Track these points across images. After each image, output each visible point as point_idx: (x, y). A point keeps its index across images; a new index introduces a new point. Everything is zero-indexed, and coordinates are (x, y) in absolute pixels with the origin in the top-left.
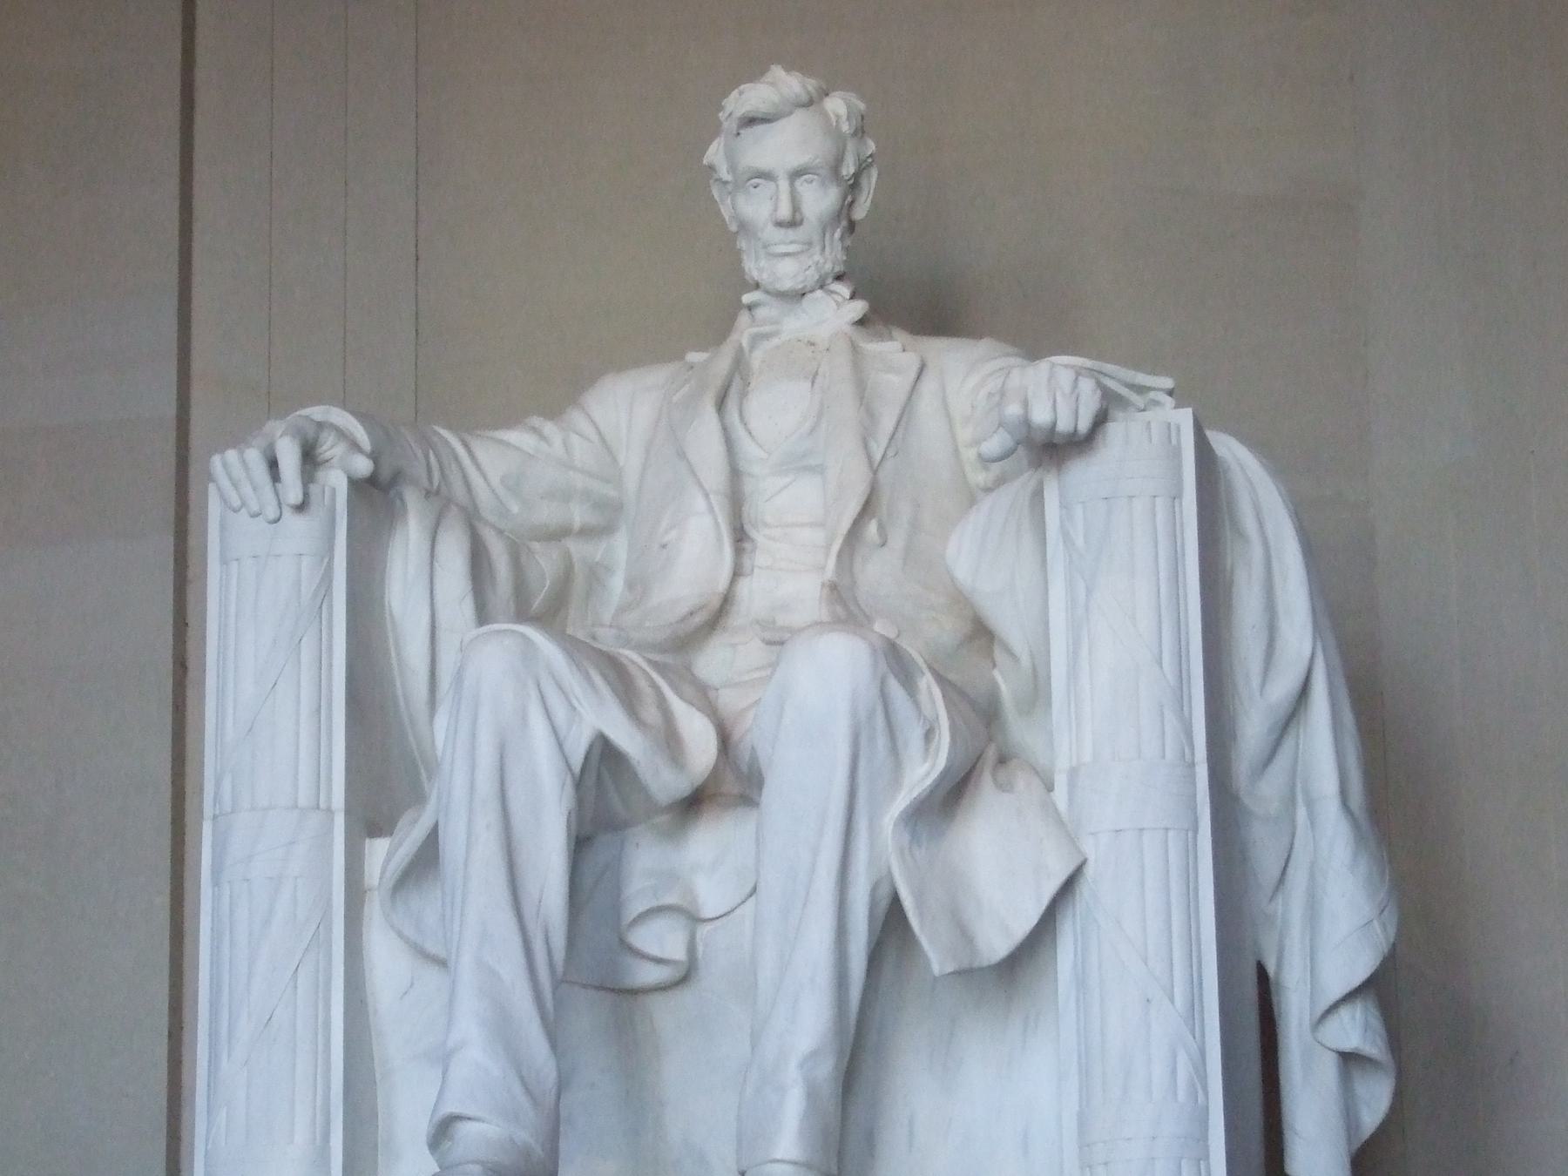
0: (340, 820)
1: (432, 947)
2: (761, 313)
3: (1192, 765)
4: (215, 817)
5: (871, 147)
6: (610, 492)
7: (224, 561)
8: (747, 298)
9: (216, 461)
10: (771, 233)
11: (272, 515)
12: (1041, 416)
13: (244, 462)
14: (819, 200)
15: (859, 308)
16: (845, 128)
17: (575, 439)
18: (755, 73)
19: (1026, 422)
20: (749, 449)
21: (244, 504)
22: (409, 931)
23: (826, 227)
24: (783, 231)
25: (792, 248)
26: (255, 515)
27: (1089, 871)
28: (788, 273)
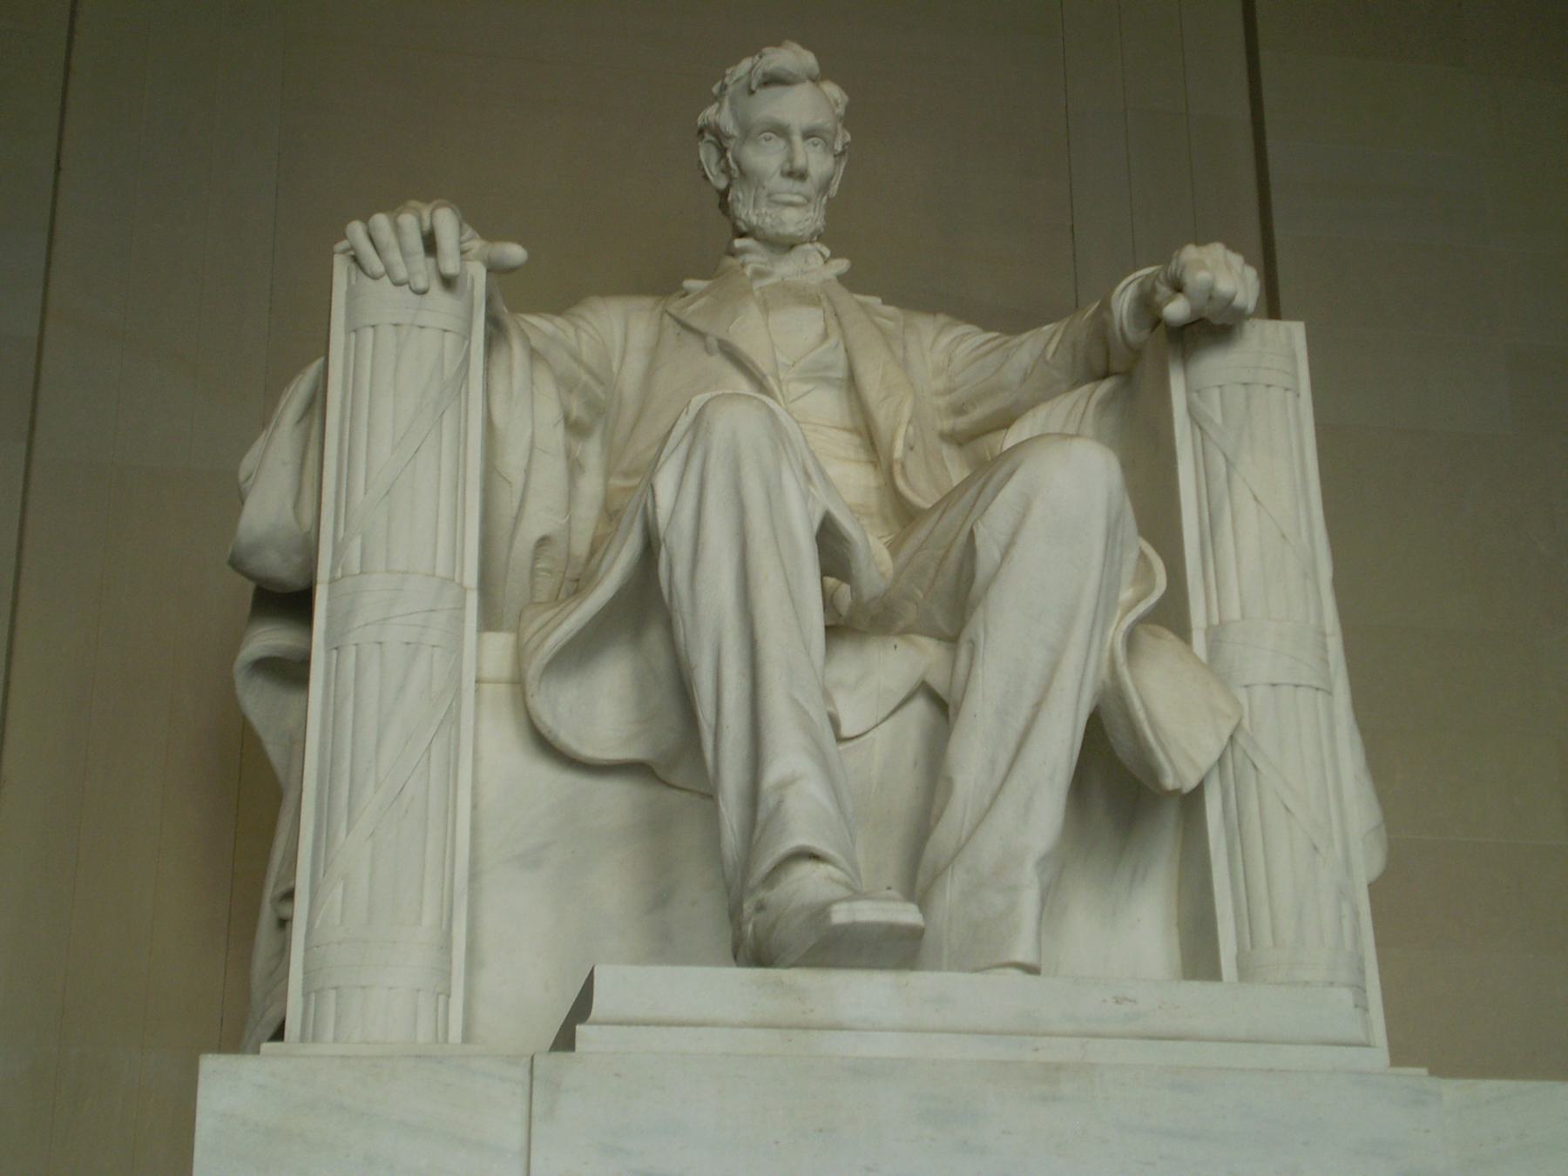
0: (473, 600)
1: (567, 738)
2: (748, 258)
3: (1324, 635)
4: (332, 581)
5: (849, 138)
6: (598, 390)
7: (353, 329)
8: (738, 243)
9: (356, 229)
10: (776, 182)
11: (421, 285)
12: (1225, 285)
13: (397, 228)
14: (818, 162)
15: (841, 265)
16: (840, 110)
17: (584, 336)
18: (778, 44)
19: (1211, 294)
20: (781, 359)
21: (388, 271)
22: (547, 719)
23: (824, 187)
24: (788, 184)
25: (797, 199)
26: (397, 284)
27: (1246, 723)
28: (793, 221)
